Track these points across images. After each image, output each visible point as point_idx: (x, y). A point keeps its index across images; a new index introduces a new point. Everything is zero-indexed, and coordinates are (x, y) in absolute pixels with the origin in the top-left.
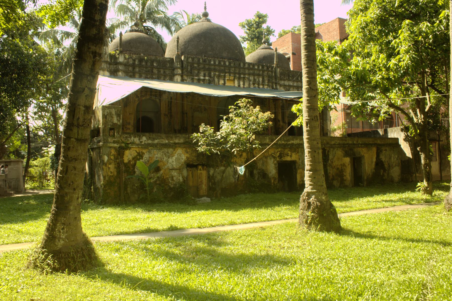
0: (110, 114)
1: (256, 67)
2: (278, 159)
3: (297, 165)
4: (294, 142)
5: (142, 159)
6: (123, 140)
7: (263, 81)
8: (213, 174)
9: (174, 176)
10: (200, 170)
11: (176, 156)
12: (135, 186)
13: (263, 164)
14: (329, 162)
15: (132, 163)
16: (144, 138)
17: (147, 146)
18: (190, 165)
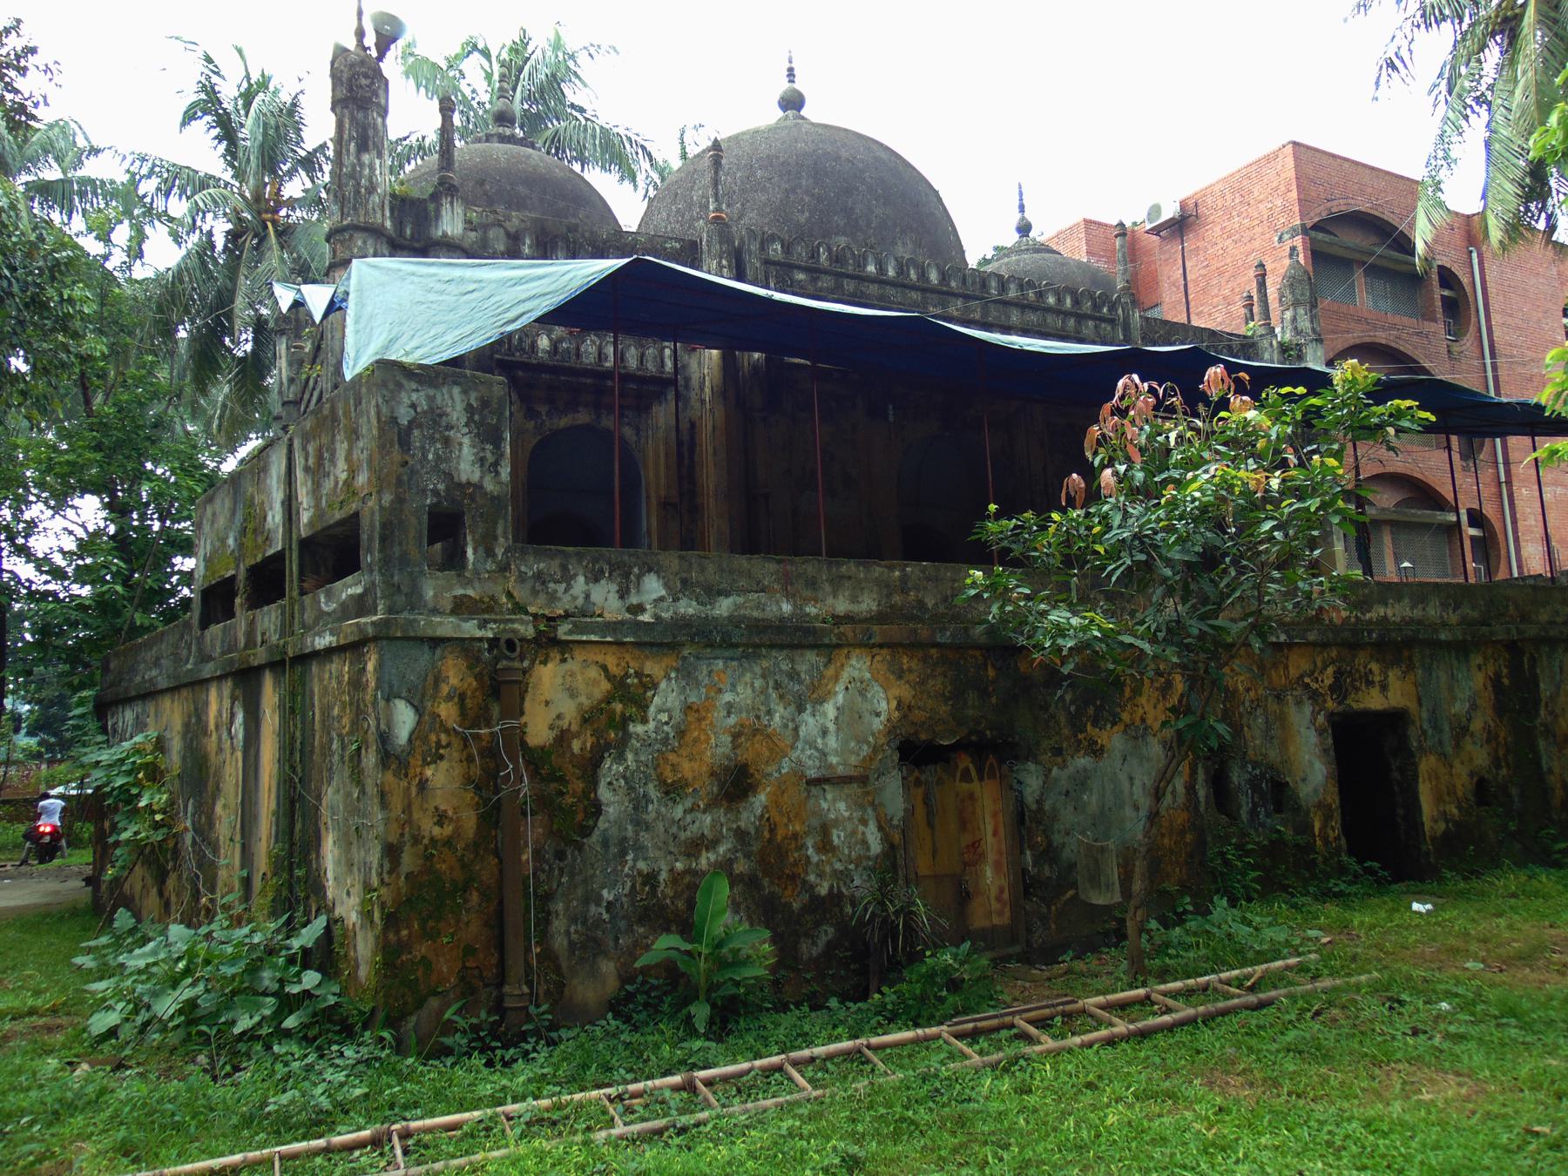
0: (435, 418)
1: (1051, 300)
2: (1330, 705)
3: (1413, 732)
4: (1390, 613)
5: (645, 721)
6: (520, 594)
8: (1039, 802)
9: (836, 823)
10: (966, 777)
11: (840, 698)
12: (598, 900)
13: (1267, 734)
14: (1542, 712)
15: (576, 745)
16: (653, 587)
17: (666, 640)
18: (915, 751)
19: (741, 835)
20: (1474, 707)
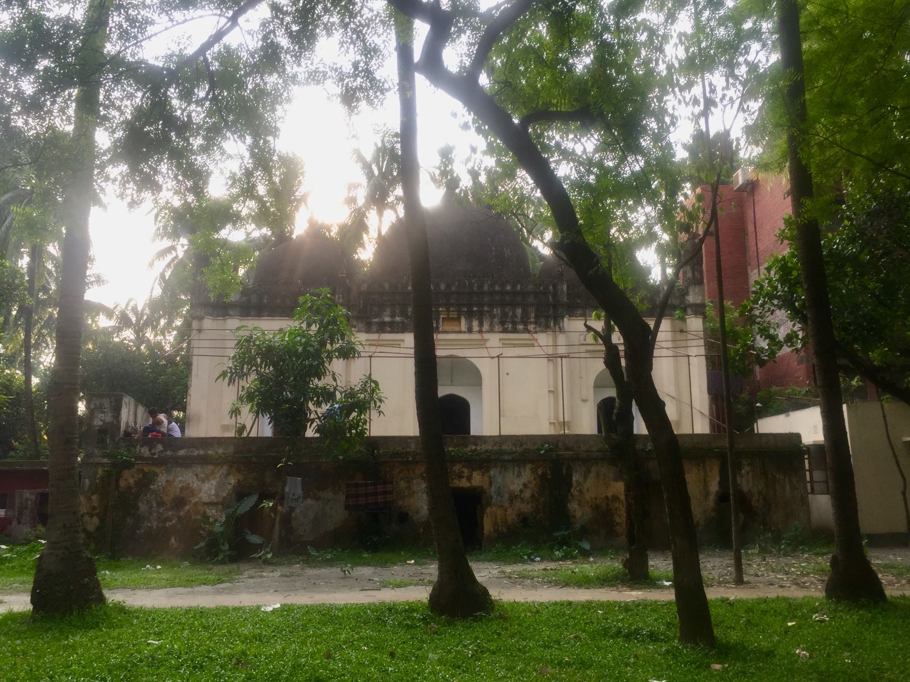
4: (478, 448)
7: (525, 315)
19: (179, 517)
20: (525, 485)
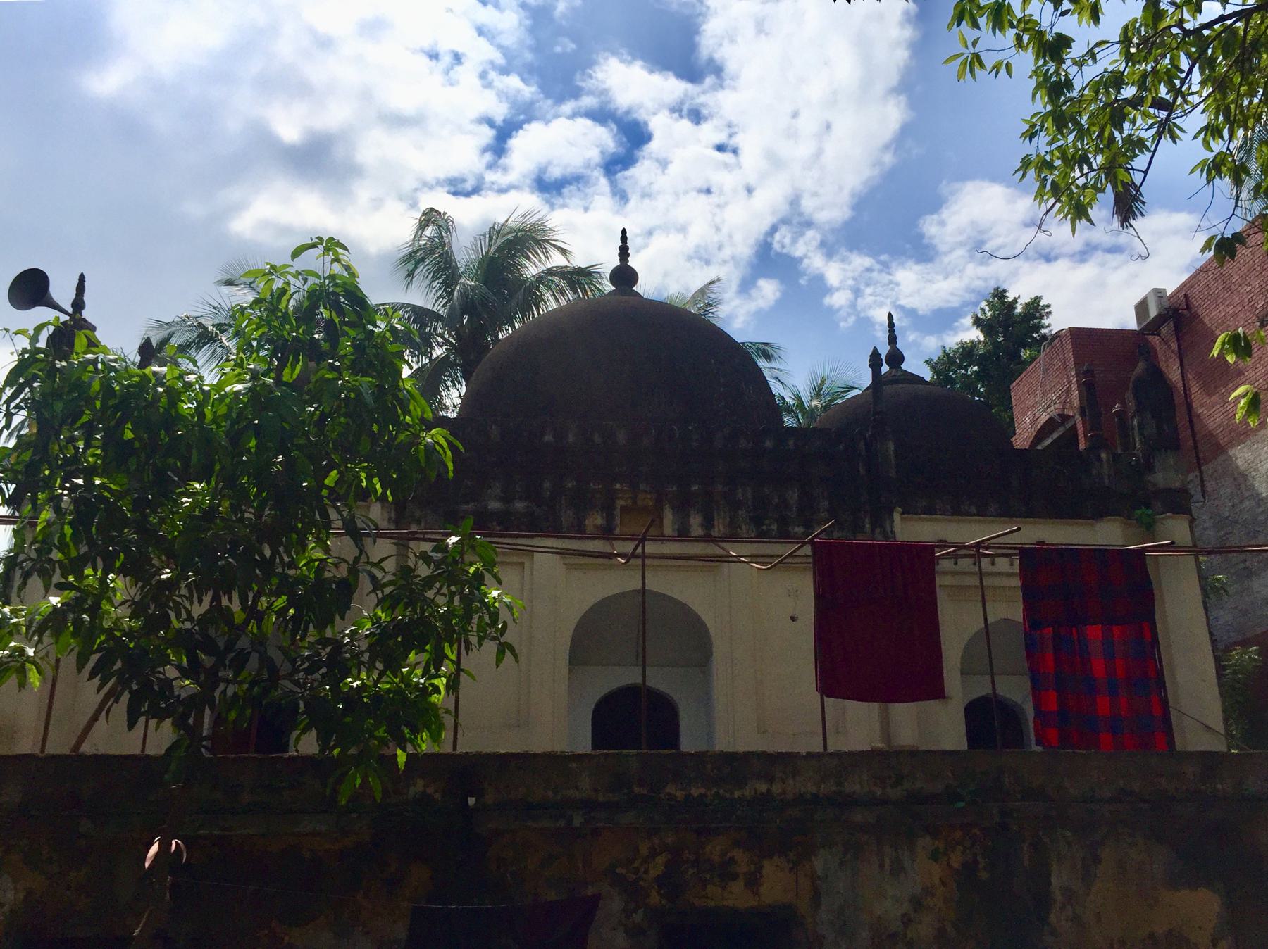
2: (655, 899)
4: (776, 788)
